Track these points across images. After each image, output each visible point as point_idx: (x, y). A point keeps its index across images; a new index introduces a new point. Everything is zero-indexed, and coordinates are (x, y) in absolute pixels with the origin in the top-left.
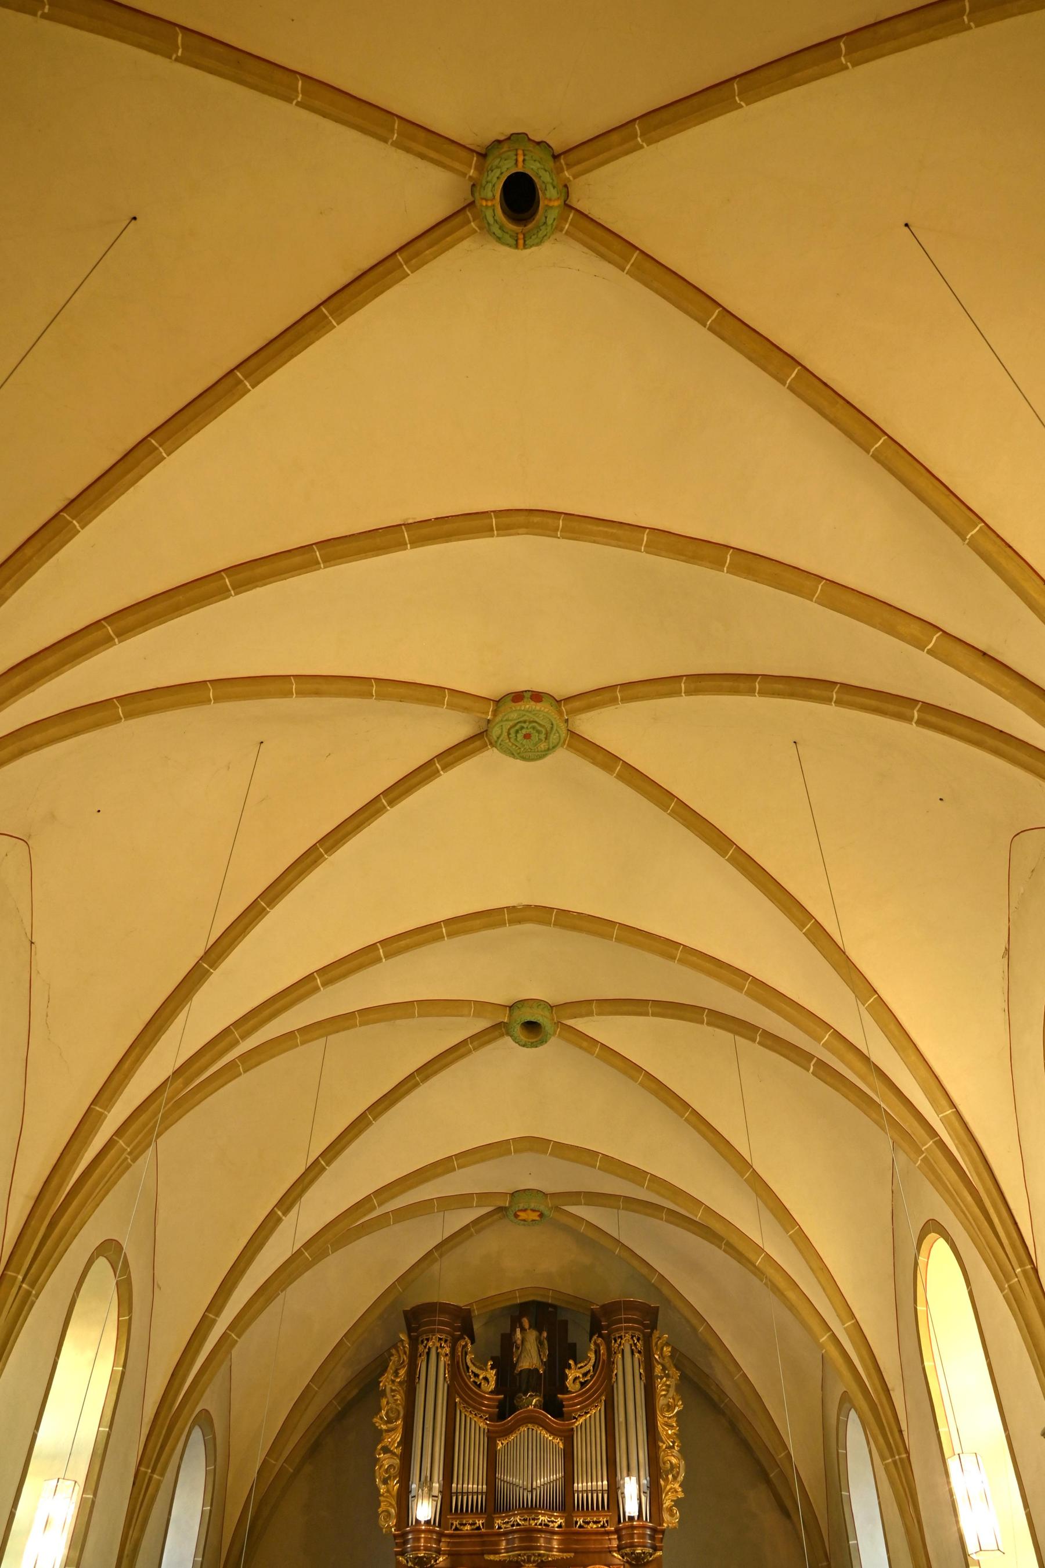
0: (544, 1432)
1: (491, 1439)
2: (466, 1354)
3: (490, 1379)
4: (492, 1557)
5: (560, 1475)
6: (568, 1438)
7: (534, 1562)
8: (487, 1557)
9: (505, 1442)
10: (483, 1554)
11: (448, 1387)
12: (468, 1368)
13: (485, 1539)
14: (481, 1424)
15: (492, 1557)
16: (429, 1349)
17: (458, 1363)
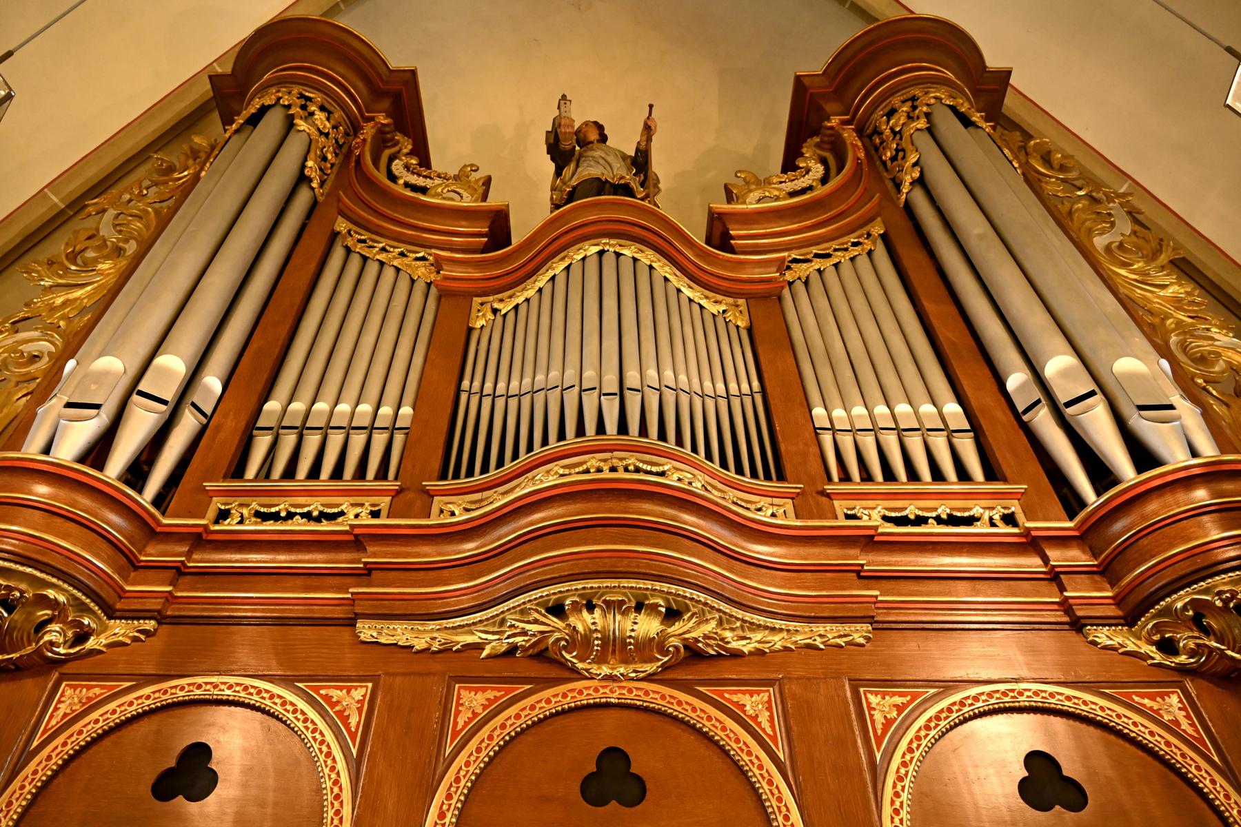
0: (664, 269)
1: (453, 299)
2: (392, 159)
3: (465, 194)
4: (400, 633)
5: (745, 384)
6: (766, 300)
7: (645, 648)
8: (367, 631)
9: (505, 308)
10: (351, 623)
11: (314, 204)
12: (393, 178)
13: (375, 555)
14: (423, 272)
15: (400, 633)
16: (264, 110)
17: (359, 160)
